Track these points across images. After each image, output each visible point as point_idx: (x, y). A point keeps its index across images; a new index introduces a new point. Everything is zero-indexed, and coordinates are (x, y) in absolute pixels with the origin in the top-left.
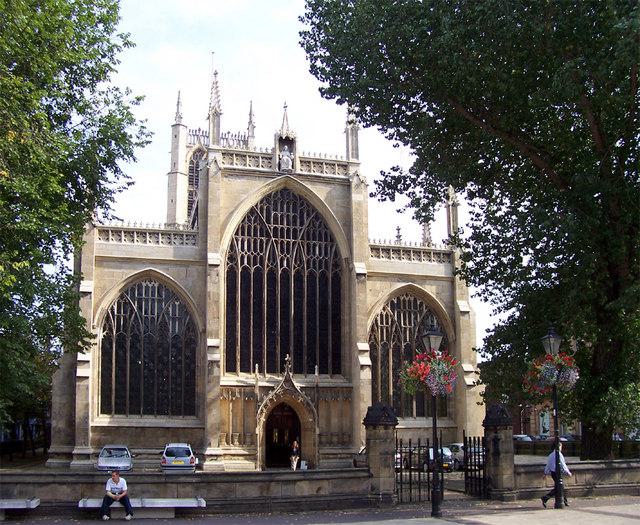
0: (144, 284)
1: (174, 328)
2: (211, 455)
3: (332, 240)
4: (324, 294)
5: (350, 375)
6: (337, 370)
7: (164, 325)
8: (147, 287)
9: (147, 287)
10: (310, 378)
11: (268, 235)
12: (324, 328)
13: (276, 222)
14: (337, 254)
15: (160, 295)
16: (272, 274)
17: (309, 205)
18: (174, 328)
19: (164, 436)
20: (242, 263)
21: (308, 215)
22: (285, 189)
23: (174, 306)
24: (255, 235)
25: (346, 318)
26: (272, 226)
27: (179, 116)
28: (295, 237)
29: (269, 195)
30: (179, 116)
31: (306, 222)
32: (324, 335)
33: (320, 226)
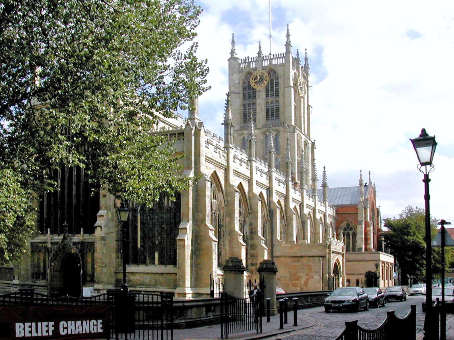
2: (14, 285)
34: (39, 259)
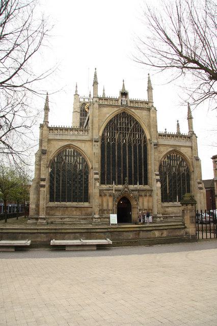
0: (67, 150)
1: (80, 167)
3: (143, 132)
4: (140, 152)
5: (151, 185)
6: (146, 183)
7: (76, 166)
8: (69, 151)
9: (69, 151)
10: (136, 186)
11: (117, 130)
12: (140, 166)
13: (120, 125)
14: (145, 137)
15: (74, 154)
16: (119, 145)
17: (133, 118)
18: (80, 167)
19: (76, 211)
20: (107, 140)
21: (133, 123)
22: (124, 112)
23: (80, 158)
24: (112, 130)
25: (150, 162)
26: (119, 126)
27: (76, 91)
28: (128, 131)
29: (118, 115)
30: (76, 91)
31: (133, 125)
32: (141, 170)
33: (138, 126)
34: (102, 202)
